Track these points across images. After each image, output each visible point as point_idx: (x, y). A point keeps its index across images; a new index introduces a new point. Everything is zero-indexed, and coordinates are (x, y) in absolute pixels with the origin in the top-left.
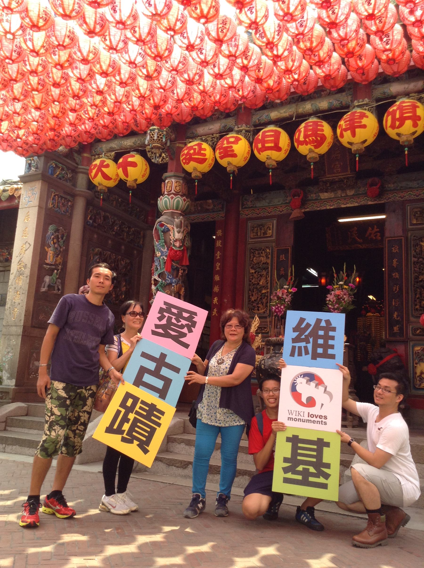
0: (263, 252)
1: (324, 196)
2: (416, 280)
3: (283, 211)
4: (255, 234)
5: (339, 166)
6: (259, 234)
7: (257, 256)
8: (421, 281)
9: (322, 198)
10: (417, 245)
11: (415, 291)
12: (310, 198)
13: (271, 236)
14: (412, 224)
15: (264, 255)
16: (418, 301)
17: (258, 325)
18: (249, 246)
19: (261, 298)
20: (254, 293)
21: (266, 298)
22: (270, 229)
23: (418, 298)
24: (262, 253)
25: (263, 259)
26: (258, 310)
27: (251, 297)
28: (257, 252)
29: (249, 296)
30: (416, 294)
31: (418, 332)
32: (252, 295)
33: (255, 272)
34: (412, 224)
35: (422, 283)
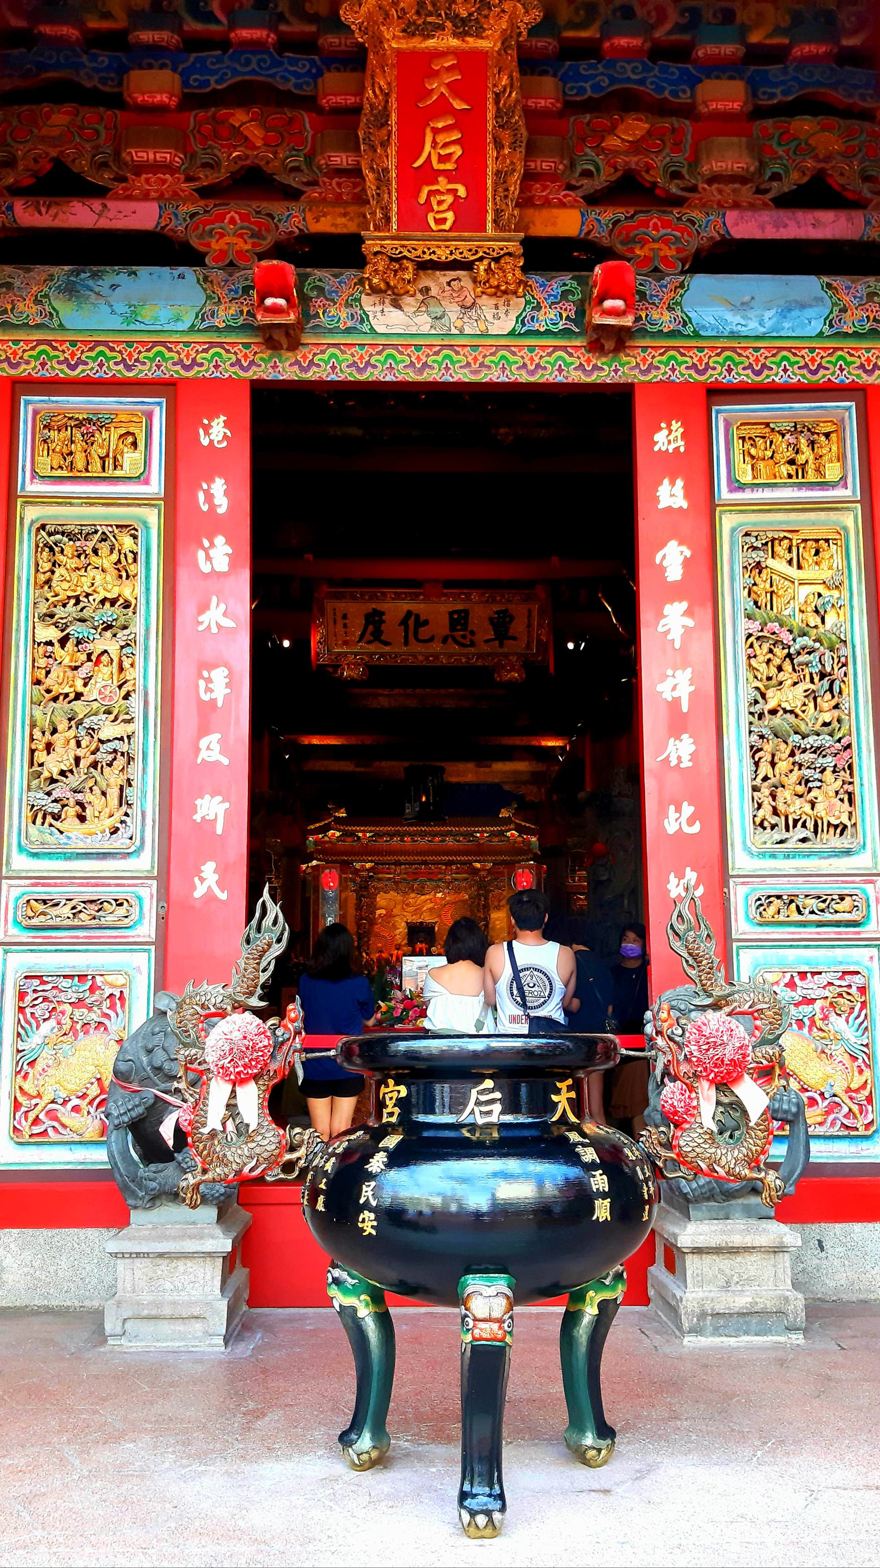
0: (104, 548)
1: (388, 320)
2: (757, 708)
3: (194, 363)
4: (57, 460)
5: (449, 199)
6: (80, 464)
7: (73, 563)
8: (773, 712)
9: (380, 329)
10: (759, 567)
11: (755, 750)
12: (324, 320)
13: (143, 479)
14: (736, 486)
15: (107, 560)
16: (766, 791)
17: (277, 950)
18: (31, 514)
19: (94, 765)
20: (58, 740)
21: (121, 762)
22: (134, 444)
23: (766, 779)
24: (95, 551)
25: (106, 585)
26: (82, 819)
27: (41, 756)
28: (69, 547)
29: (32, 752)
30: (757, 764)
31: (772, 910)
32: (49, 747)
33: (63, 642)
34: (736, 486)
35: (777, 720)
